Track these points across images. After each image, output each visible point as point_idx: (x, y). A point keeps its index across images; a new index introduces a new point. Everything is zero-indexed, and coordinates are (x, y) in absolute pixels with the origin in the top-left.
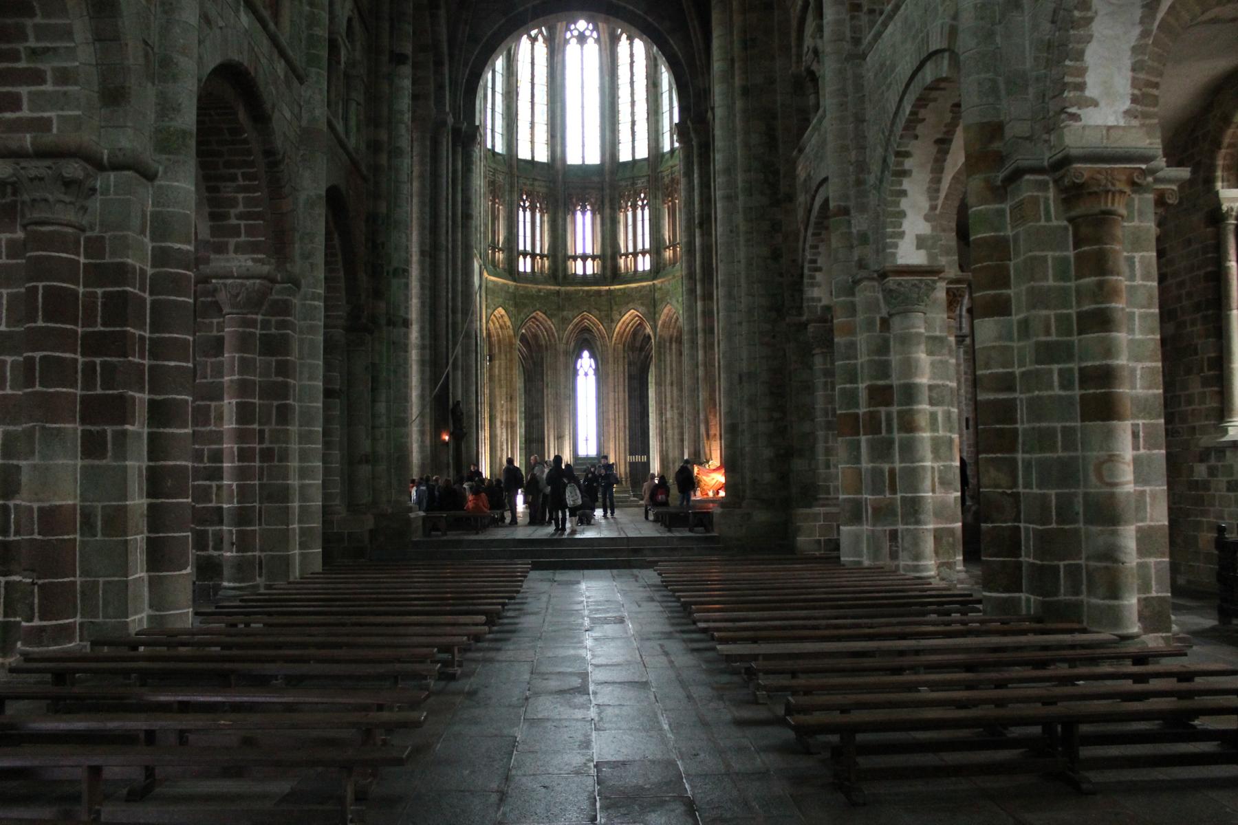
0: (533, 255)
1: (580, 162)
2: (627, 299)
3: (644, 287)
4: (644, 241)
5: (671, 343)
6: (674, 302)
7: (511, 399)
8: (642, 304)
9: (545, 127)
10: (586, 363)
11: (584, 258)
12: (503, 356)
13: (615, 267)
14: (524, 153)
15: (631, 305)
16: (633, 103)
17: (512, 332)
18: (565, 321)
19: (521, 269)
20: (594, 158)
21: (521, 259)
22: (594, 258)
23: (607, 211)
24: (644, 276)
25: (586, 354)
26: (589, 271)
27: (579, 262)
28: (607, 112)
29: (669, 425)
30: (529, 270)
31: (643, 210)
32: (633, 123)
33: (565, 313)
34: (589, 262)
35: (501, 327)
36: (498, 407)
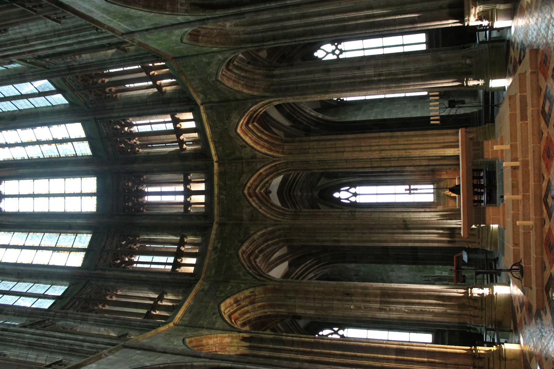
0: (179, 254)
1: (95, 198)
2: (226, 138)
3: (208, 118)
4: (161, 123)
5: (273, 76)
6: (212, 69)
7: (348, 294)
8: (229, 118)
9: (63, 236)
10: (343, 195)
11: (188, 193)
12: (290, 302)
13: (195, 155)
14: (76, 260)
15: (232, 134)
16: (39, 143)
17: (258, 289)
18: (254, 217)
19: (191, 270)
20: (90, 184)
22: (187, 182)
23: (136, 166)
24: (197, 119)
25: (336, 195)
26: (202, 187)
27: (195, 199)
28: (49, 170)
29: (385, 70)
30: (193, 261)
31: (131, 125)
32: (56, 141)
33: (245, 216)
34: (195, 187)
35: (252, 303)
36: (359, 313)
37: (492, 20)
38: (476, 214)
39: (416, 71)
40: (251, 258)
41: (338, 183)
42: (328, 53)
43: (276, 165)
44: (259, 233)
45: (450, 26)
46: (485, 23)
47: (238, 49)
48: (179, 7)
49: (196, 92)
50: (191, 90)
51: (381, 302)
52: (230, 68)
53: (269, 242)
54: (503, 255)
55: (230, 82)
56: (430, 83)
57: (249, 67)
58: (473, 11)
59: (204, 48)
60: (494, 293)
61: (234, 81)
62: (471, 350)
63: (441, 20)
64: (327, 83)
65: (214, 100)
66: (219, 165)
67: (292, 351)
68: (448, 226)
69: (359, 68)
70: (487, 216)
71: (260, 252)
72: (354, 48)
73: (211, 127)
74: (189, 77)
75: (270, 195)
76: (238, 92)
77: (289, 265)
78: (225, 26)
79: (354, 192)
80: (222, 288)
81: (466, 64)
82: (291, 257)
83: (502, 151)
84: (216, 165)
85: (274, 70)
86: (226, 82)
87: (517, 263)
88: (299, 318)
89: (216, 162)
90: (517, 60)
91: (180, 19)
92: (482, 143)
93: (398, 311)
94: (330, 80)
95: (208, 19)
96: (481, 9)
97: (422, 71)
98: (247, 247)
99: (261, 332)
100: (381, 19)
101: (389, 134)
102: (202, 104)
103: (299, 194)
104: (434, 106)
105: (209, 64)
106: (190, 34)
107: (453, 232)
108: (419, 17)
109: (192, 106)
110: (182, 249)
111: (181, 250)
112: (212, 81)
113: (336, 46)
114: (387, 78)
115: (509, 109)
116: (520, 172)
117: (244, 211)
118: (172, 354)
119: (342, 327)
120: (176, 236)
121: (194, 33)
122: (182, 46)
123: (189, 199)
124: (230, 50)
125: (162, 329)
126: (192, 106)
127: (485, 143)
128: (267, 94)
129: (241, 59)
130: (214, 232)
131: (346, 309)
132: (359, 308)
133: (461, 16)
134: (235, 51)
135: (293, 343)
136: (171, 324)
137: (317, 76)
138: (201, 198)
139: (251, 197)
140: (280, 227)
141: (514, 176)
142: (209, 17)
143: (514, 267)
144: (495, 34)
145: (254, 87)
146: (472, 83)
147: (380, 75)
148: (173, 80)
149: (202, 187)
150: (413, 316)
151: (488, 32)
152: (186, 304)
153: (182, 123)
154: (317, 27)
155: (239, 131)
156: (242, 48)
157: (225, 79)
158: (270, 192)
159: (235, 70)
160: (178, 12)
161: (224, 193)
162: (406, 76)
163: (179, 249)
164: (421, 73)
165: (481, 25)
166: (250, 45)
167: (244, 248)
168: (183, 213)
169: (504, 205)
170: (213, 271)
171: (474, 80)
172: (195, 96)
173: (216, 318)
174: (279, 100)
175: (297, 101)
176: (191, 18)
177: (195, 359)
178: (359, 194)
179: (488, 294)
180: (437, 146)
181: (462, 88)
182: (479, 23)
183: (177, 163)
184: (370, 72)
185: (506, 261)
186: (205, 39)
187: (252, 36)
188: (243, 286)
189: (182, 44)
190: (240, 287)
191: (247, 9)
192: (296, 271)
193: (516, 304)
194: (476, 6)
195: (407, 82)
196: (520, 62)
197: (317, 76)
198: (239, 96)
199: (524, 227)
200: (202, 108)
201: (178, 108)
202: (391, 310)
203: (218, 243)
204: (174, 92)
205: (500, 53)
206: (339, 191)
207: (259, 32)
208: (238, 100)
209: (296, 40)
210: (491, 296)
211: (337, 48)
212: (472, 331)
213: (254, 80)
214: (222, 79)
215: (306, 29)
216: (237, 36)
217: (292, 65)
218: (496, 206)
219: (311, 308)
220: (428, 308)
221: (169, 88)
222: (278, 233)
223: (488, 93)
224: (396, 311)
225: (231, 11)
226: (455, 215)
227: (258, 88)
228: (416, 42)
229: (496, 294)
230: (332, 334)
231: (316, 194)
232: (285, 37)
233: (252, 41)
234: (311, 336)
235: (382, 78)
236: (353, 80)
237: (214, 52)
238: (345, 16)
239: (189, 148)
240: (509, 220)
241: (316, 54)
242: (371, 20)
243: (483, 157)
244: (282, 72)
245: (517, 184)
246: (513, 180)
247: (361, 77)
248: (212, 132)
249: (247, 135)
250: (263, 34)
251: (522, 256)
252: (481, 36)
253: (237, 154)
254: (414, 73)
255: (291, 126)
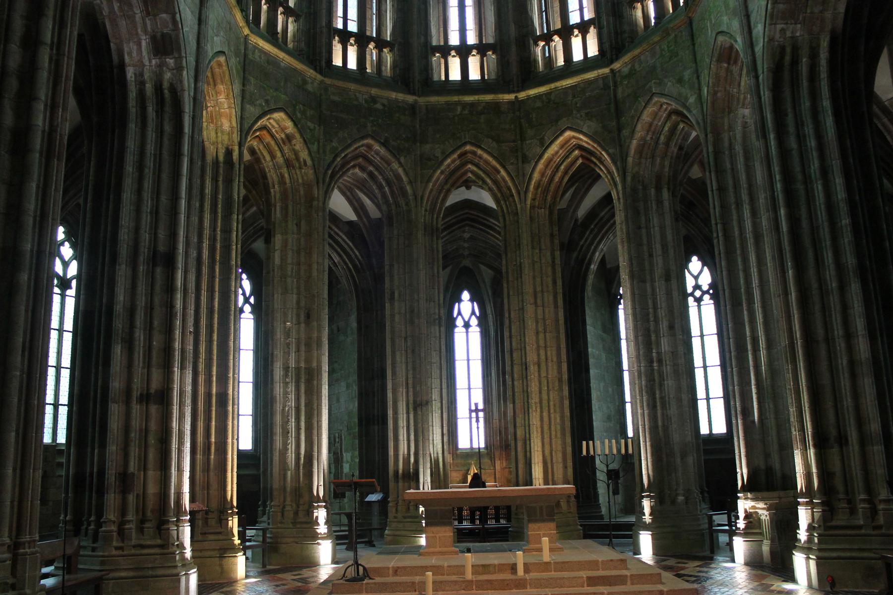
0: (362, 39)
2: (556, 112)
3: (589, 82)
5: (659, 189)
6: (670, 86)
8: (589, 116)
10: (466, 306)
11: (464, 51)
12: (291, 226)
13: (528, 62)
15: (563, 123)
17: (311, 172)
18: (428, 163)
19: (338, 61)
21: (337, 49)
22: (482, 49)
24: (588, 64)
25: (466, 295)
26: (474, 74)
27: (455, 64)
29: (668, 369)
30: (352, 64)
33: (427, 147)
34: (474, 62)
35: (288, 163)
36: (279, 335)
37: (746, 533)
38: (442, 512)
39: (667, 418)
40: (360, 160)
41: (485, 297)
42: (696, 278)
43: (513, 196)
44: (400, 171)
45: (738, 470)
46: (741, 524)
47: (705, 130)
48: (779, 27)
49: (633, 59)
50: (636, 52)
51: (298, 369)
52: (674, 117)
53: (387, 189)
54: (379, 553)
55: (650, 116)
56: (648, 440)
57: (674, 149)
58: (761, 505)
59: (706, 72)
60: (319, 541)
61: (651, 125)
62: (232, 507)
63: (747, 456)
64: (648, 277)
65: (620, 90)
66: (511, 103)
67: (215, 230)
68: (421, 470)
69: (671, 327)
70: (438, 528)
71: (371, 174)
72: (703, 319)
73: (573, 87)
74: (658, 47)
75: (464, 188)
76: (633, 132)
77: (352, 222)
78: (743, 106)
79: (471, 323)
80: (309, 113)
81: (677, 495)
82: (364, 224)
83: (540, 550)
84: (512, 97)
85: (669, 189)
86: (650, 109)
87: (367, 573)
88: (268, 241)
89: (516, 97)
90: (682, 572)
91: (759, 29)
92: (553, 520)
93: (286, 396)
94: (653, 281)
95: (757, 77)
96: (763, 517)
97: (666, 428)
98: (377, 153)
99: (242, 180)
100: (751, 363)
101: (565, 377)
102: (612, 71)
103: (466, 236)
104: (610, 448)
105: (680, 81)
106: (731, 47)
107: (412, 477)
108: (754, 421)
109: (608, 55)
110: (371, 46)
111: (368, 43)
112: (651, 87)
113: (707, 292)
114: (656, 374)
115: (605, 559)
116: (507, 576)
117: (437, 146)
118: (199, 33)
119: (256, 310)
120: (393, 34)
121: (733, 55)
122: (711, 34)
123: (453, 53)
124: (703, 116)
125: (239, 16)
126: (608, 55)
127: (552, 525)
128: (629, 179)
129: (688, 135)
130: (401, 96)
131: (285, 315)
132: (287, 334)
133: (754, 487)
134: (702, 124)
135: (227, 231)
136: (246, 31)
137: (659, 261)
138: (455, 75)
139: (460, 156)
140: (412, 204)
141: (501, 568)
142: (761, 78)
143: (361, 568)
144: (723, 538)
145: (640, 157)
146: (647, 504)
147: (660, 361)
148: (653, 21)
149: (474, 74)
150: (278, 419)
151: (727, 528)
152: (281, 55)
153: (580, 38)
154: (739, 260)
155: (568, 134)
156: (706, 136)
157: (655, 109)
158: (468, 188)
159: (668, 125)
160: (771, 24)
161: (466, 112)
162: (658, 404)
163: (371, 39)
164: (664, 425)
165: (737, 518)
166: (711, 149)
167: (377, 147)
168: (431, 43)
169: (456, 553)
170: (336, 98)
171: (652, 507)
172: (627, 58)
173: (261, 105)
174: (619, 198)
175: (618, 227)
176: (759, 49)
177: (192, 73)
178: (467, 332)
179: (319, 531)
180: (547, 453)
181: (638, 489)
182: (741, 514)
183: (513, 30)
184: (665, 345)
185: (369, 558)
186: (723, 73)
187: (727, 152)
188: (315, 147)
189: (714, 35)
190: (313, 144)
191: (773, 143)
192: (341, 234)
193: (305, 573)
194: (768, 509)
195: (648, 405)
196: (679, 576)
197: (659, 261)
198: (625, 132)
199: (424, 583)
200: (606, 70)
201: (605, 30)
202: (286, 384)
203: (384, 105)
204: (633, 23)
205: (692, 547)
206: (472, 300)
207: (732, 164)
208: (619, 130)
209: (719, 226)
210: (315, 536)
211: (704, 293)
212: (260, 509)
213: (653, 157)
214: (655, 104)
215: (738, 241)
216: (726, 128)
217: (677, 220)
218: (454, 542)
219: (283, 259)
220: (292, 441)
221: (639, 13)
222: (402, 202)
223: (631, 531)
224: (286, 393)
225: (769, 116)
226: (439, 479)
227: (640, 163)
228: (713, 419)
229: (318, 544)
230: (244, 294)
231: (467, 263)
232: (724, 207)
233: (718, 153)
234: (239, 260)
235: (655, 364)
236: (652, 319)
237: (700, 89)
238: (757, 305)
239: (539, 51)
240: (433, 561)
241: (695, 259)
242: (749, 347)
243: (530, 521)
244: (666, 204)
245: (489, 573)
246: (495, 566)
247: (657, 332)
248: (566, 90)
249: (562, 146)
250: (729, 171)
251: (378, 580)
252: (720, 519)
253: (530, 132)
254: (663, 414)
255: (576, 220)
